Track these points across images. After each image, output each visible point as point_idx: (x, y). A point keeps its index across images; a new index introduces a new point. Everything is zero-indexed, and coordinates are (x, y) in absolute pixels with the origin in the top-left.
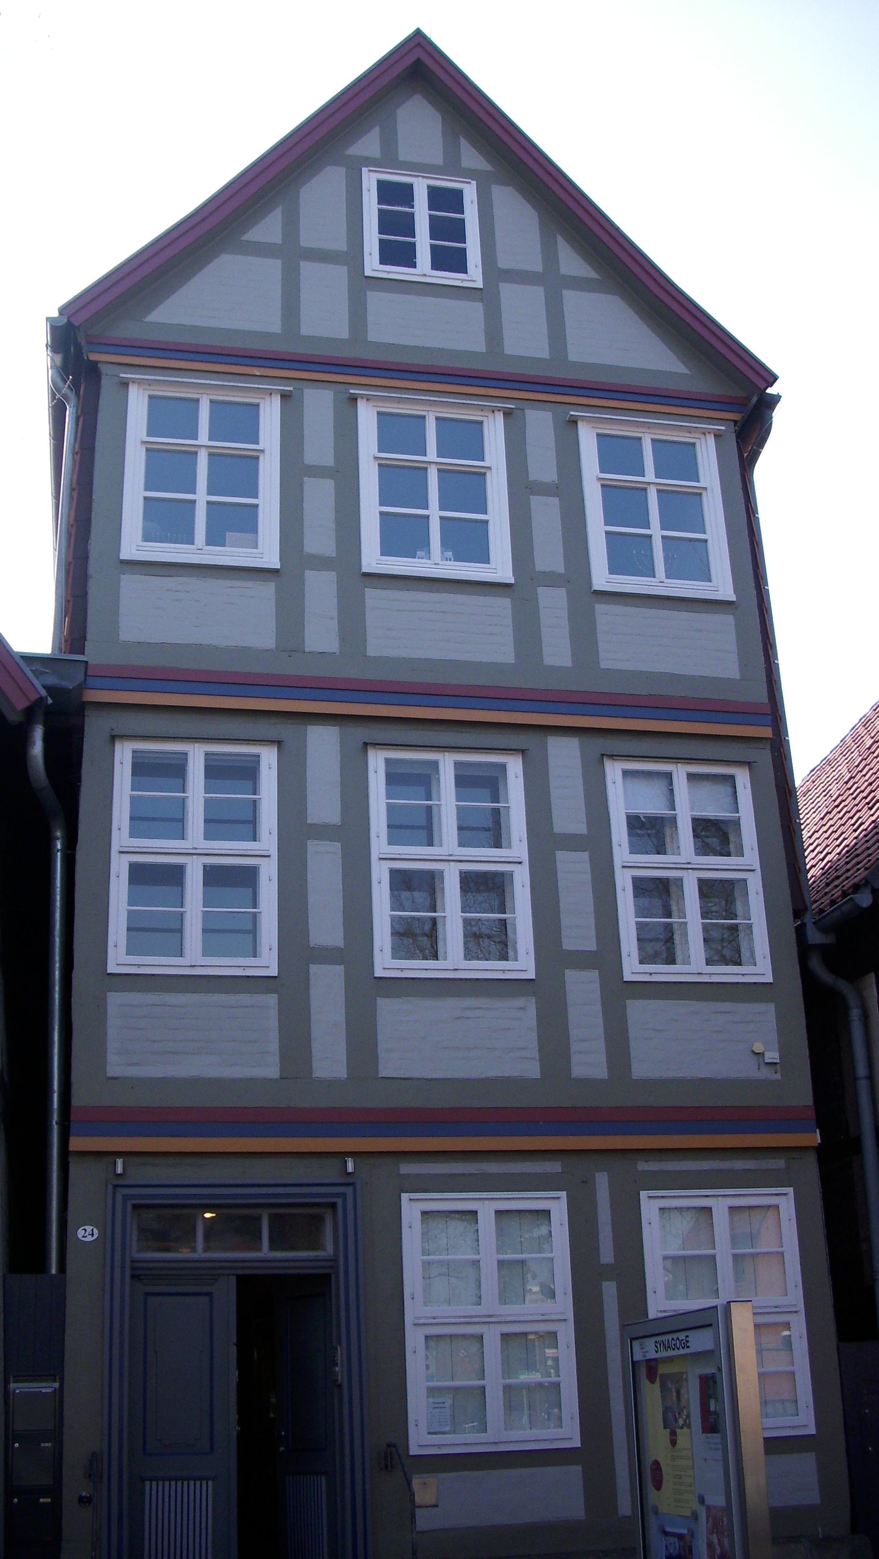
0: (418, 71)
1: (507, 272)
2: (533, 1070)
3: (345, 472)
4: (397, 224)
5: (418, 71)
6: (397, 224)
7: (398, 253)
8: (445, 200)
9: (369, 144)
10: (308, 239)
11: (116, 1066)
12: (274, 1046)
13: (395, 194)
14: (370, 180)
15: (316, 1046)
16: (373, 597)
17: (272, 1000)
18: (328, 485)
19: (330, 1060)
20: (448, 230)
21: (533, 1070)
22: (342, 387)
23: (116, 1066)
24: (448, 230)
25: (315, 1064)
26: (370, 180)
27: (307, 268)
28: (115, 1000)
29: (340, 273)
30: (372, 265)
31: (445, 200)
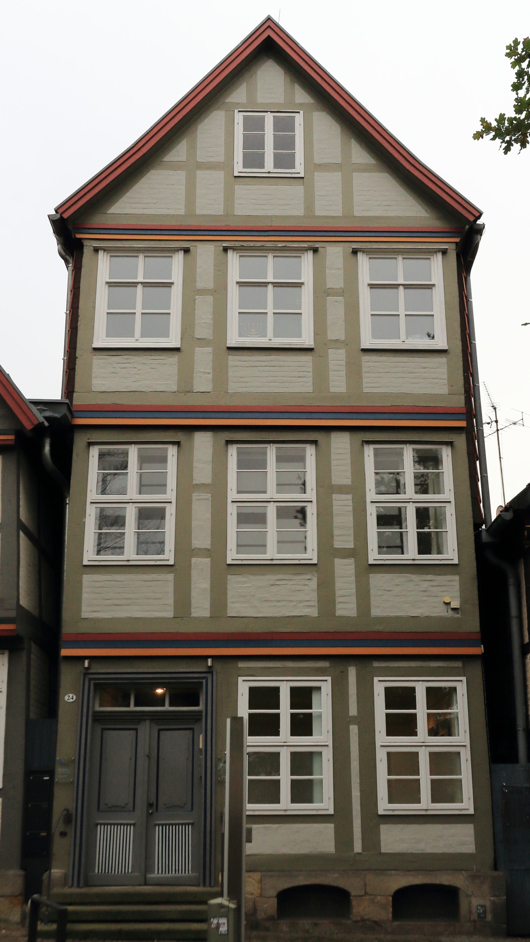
0: (269, 47)
1: (320, 165)
2: (313, 612)
3: (219, 291)
4: (253, 144)
5: (269, 47)
6: (253, 144)
7: (254, 159)
8: (284, 126)
9: (239, 95)
10: (201, 156)
11: (86, 612)
12: (171, 601)
13: (254, 125)
14: (239, 118)
15: (193, 601)
16: (234, 360)
17: (171, 577)
18: (210, 299)
19: (201, 607)
20: (284, 143)
21: (313, 612)
22: (219, 243)
23: (86, 612)
24: (284, 143)
25: (193, 610)
26: (239, 118)
27: (200, 174)
28: (87, 579)
29: (220, 175)
30: (238, 168)
31: (284, 126)
